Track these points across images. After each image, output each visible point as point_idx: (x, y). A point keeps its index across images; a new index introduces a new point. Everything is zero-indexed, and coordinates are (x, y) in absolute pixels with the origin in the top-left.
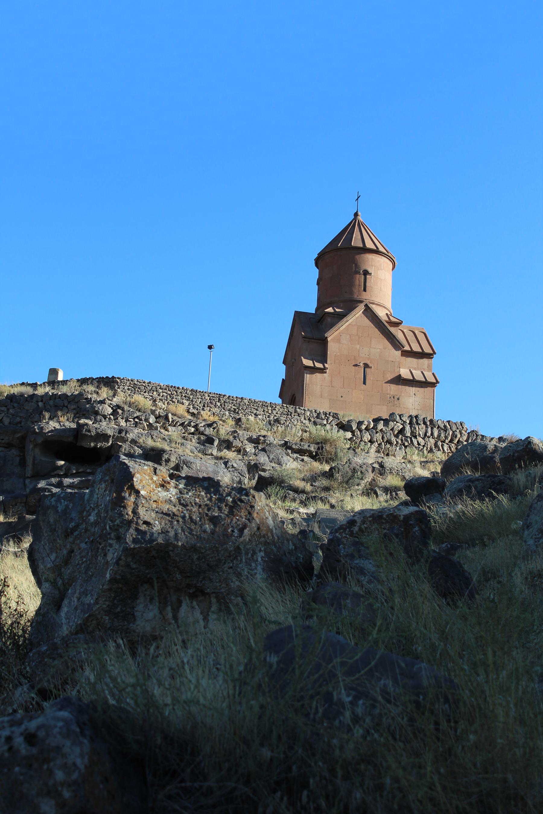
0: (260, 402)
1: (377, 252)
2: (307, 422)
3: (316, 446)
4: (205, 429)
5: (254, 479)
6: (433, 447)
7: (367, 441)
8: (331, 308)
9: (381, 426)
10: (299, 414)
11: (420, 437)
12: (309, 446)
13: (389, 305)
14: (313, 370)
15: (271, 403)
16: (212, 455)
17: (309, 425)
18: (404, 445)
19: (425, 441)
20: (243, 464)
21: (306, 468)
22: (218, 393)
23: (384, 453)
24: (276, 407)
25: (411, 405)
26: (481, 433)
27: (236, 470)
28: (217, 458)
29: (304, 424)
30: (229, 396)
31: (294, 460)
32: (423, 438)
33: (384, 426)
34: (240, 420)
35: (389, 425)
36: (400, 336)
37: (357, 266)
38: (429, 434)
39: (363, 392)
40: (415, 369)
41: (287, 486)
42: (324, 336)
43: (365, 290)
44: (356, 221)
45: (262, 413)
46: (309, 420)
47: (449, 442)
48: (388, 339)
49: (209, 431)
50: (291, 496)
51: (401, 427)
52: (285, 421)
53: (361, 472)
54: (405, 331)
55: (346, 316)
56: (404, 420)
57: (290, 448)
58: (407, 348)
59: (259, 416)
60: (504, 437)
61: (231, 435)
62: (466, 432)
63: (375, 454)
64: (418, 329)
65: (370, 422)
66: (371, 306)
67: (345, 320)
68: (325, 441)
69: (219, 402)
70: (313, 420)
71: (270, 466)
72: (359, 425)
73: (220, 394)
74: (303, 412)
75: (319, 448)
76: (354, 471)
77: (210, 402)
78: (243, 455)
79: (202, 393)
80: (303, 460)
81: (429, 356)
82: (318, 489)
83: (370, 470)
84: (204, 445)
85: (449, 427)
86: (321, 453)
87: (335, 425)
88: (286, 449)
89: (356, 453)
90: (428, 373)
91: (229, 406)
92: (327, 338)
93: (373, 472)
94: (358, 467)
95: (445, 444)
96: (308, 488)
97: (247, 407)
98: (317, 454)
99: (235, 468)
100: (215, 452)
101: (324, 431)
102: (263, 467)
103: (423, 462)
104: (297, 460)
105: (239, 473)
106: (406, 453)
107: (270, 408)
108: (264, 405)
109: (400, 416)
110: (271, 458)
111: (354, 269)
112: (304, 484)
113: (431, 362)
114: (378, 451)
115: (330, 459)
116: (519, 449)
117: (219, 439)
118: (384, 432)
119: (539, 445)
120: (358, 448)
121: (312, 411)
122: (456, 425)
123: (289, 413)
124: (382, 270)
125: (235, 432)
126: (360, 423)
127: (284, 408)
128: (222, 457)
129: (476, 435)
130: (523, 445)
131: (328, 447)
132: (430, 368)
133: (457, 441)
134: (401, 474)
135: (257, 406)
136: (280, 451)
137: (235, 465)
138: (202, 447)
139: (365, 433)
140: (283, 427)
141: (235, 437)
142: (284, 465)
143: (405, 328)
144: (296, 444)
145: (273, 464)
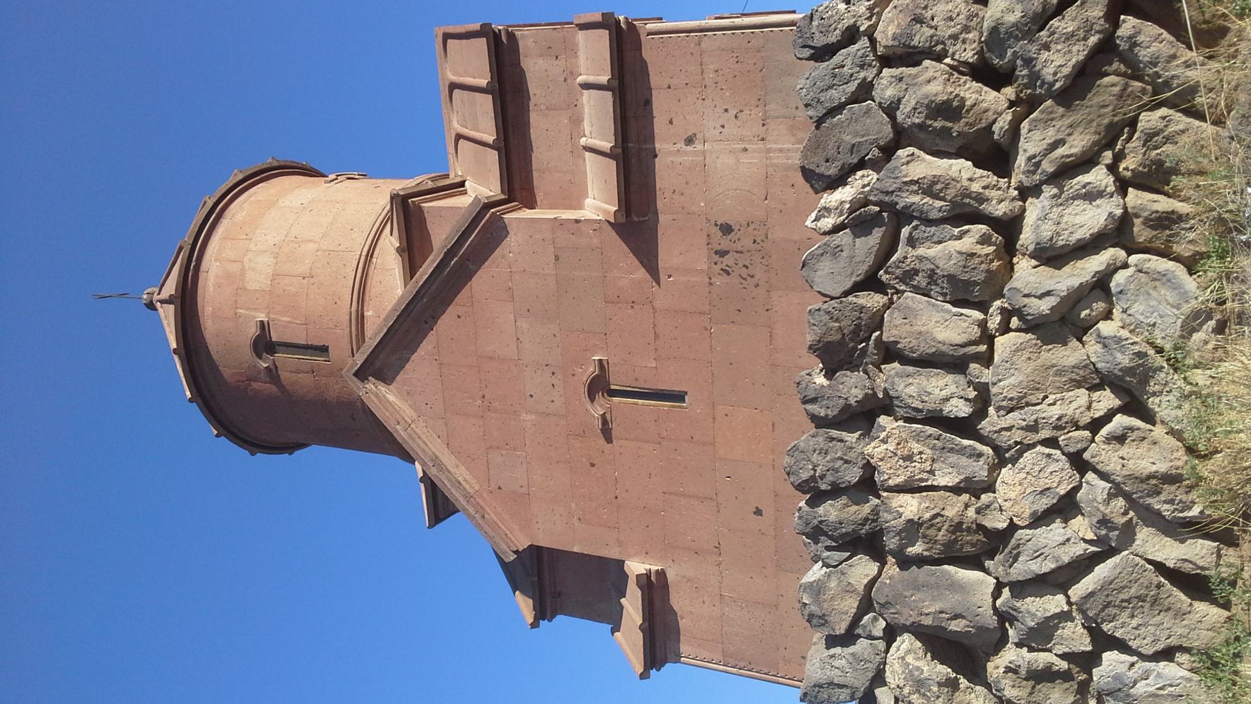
1: (186, 300)
25: (745, 159)
32: (1002, 457)
43: (323, 350)
56: (851, 604)
113: (530, 42)
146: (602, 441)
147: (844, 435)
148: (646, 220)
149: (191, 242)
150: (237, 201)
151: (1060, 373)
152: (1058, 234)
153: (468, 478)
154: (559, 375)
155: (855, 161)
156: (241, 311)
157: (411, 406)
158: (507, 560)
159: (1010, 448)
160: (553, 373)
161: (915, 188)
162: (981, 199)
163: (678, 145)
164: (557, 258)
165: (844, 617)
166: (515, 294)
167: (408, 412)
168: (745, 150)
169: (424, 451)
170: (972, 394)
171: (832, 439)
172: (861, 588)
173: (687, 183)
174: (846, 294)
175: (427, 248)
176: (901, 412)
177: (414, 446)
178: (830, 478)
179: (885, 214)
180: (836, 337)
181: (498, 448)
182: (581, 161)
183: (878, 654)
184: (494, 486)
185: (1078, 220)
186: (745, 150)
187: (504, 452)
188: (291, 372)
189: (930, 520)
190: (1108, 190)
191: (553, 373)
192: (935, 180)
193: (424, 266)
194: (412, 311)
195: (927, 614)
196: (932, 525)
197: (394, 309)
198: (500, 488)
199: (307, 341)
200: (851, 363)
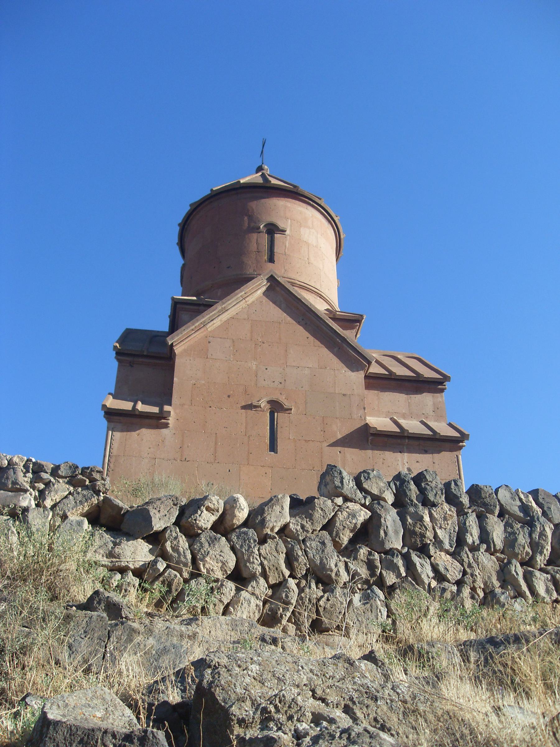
6: (497, 584)
11: (442, 549)
19: (462, 563)
32: (455, 554)
35: (313, 509)
39: (269, 471)
40: (404, 417)
43: (271, 259)
51: (363, 515)
56: (375, 491)
65: (235, 500)
72: (187, 513)
85: (539, 511)
90: (436, 423)
111: (246, 224)
118: (295, 537)
124: (309, 228)
139: (212, 542)
146: (244, 404)
147: (444, 496)
148: (368, 443)
149: (322, 204)
150: (333, 232)
151: (489, 578)
152: (537, 579)
153: (215, 325)
154: (280, 386)
155: (545, 509)
156: (289, 221)
157: (253, 302)
158: (168, 339)
159: (461, 557)
160: (281, 383)
161: (542, 529)
162: (541, 553)
163: (407, 464)
164: (344, 395)
165: (370, 487)
166: (323, 370)
167: (250, 300)
169: (230, 304)
170: (476, 544)
171: (442, 491)
172: (383, 496)
173: (389, 466)
174: (499, 501)
176: (461, 518)
177: (233, 299)
178: (428, 487)
179: (529, 518)
180: (483, 496)
181: (234, 345)
182: (385, 416)
183: (359, 499)
185: (541, 586)
187: (231, 348)
189: (424, 525)
190: (552, 597)
191: (281, 383)
192: (546, 536)
193: (336, 324)
194: (309, 313)
195: (385, 521)
196: (421, 526)
197: (314, 306)
198: (209, 342)
199: (277, 253)
200: (471, 501)
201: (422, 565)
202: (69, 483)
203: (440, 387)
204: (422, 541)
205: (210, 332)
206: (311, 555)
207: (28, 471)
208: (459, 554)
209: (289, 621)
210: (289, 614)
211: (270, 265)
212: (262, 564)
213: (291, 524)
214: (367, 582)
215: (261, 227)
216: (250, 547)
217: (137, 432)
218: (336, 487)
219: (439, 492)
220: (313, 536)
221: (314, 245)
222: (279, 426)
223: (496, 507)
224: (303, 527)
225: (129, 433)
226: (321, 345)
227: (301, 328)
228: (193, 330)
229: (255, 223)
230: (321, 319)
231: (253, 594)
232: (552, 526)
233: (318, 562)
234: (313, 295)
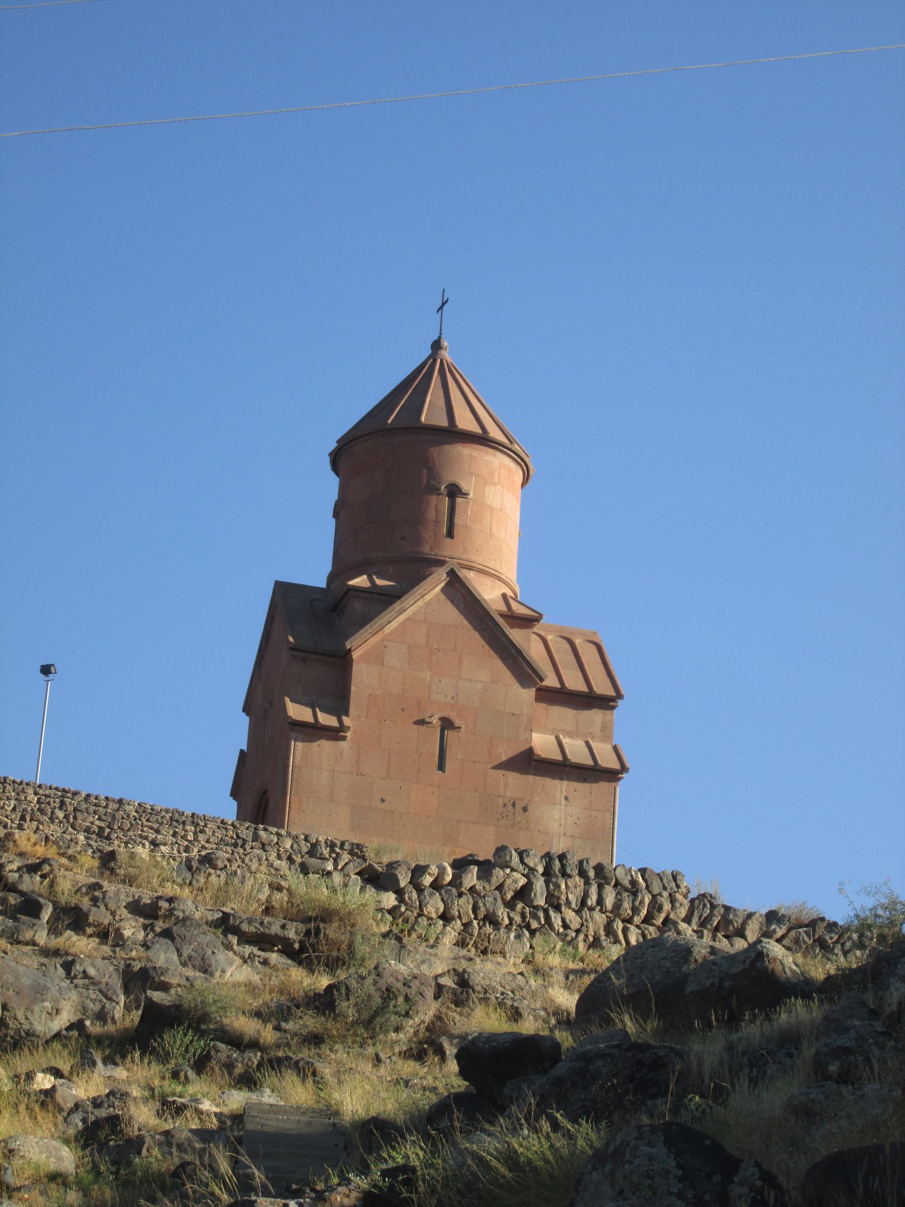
0: (167, 811)
1: (483, 440)
2: (283, 864)
3: (302, 927)
4: (21, 876)
5: (137, 1008)
6: (602, 933)
7: (434, 915)
8: (365, 577)
9: (471, 878)
10: (263, 845)
11: (570, 907)
12: (283, 927)
13: (510, 571)
14: (313, 731)
15: (193, 815)
16: (34, 944)
17: (287, 872)
18: (528, 927)
19: (581, 918)
20: (111, 968)
21: (274, 982)
22: (61, 787)
23: (476, 947)
24: (205, 826)
25: (556, 824)
26: (725, 899)
27: (94, 984)
28: (47, 952)
29: (276, 869)
30: (88, 796)
31: (245, 962)
32: (578, 912)
33: (478, 878)
34: (112, 855)
35: (491, 875)
36: (534, 651)
37: (434, 474)
38: (592, 900)
40: (570, 735)
41: (215, 1030)
42: (344, 647)
43: (450, 534)
44: (435, 361)
45: (171, 839)
46: (290, 859)
47: (643, 922)
48: (504, 659)
49: (31, 884)
50: (223, 1056)
51: (523, 881)
52: (229, 860)
53: (407, 999)
54: (549, 638)
55: (399, 597)
56: (531, 865)
57: (236, 931)
58: (551, 681)
59: (162, 848)
60: (783, 911)
61: (87, 893)
62: (685, 896)
63: (451, 950)
64: (582, 634)
65: (444, 869)
66: (464, 574)
67: (397, 608)
68: (326, 915)
69: (61, 808)
70: (298, 859)
71: (181, 975)
73: (64, 790)
74: (275, 840)
75: (308, 933)
76: (388, 994)
77: (39, 810)
78: (113, 946)
79: (20, 787)
80: (265, 962)
81: (606, 703)
82: (292, 1039)
83: (430, 993)
84: (15, 919)
86: (313, 945)
87: (357, 874)
88: (225, 933)
89: (403, 947)
91: (85, 820)
92: (349, 651)
93: (437, 997)
94: (399, 985)
95: (632, 928)
96: (268, 1035)
97: (132, 825)
98: (303, 949)
99: (90, 978)
100: (42, 937)
101: (325, 890)
102: (162, 978)
103: (573, 971)
104: (253, 961)
105: (100, 991)
106: (531, 947)
107: (188, 828)
108: (176, 819)
109: (521, 854)
110: (185, 955)
112: (258, 1027)
113: (609, 717)
114: (461, 943)
115: (337, 959)
116: (734, 970)
117: (55, 904)
118: (478, 894)
119: (785, 962)
120: (409, 935)
121: (297, 837)
122: (662, 881)
123: (240, 842)
124: (494, 484)
125: (98, 887)
126: (418, 871)
127: (226, 829)
128: (58, 950)
129: (712, 905)
130: (744, 962)
131: (331, 931)
132: (606, 733)
133: (661, 920)
134: (509, 1002)
135: (157, 821)
136: (210, 937)
137: (92, 972)
138: (10, 923)
139: (431, 895)
140: (223, 875)
141: (95, 901)
142: (218, 974)
143: (550, 632)
144: (250, 921)
145: (190, 972)
146: (416, 719)
157: (431, 599)
162: (638, 915)
164: (513, 714)
168: (561, 825)
172: (537, 868)
175: (512, 626)
184: (387, 643)
186: (561, 825)
187: (407, 655)
188: (436, 506)
200: (596, 874)
201: (555, 918)
202: (349, 853)
203: (611, 704)
204: (558, 901)
205: (387, 635)
206: (488, 906)
207: (327, 846)
208: (581, 912)
209: (472, 946)
210: (472, 942)
211: (448, 540)
212: (459, 911)
213: (477, 887)
214: (519, 926)
215: (442, 488)
216: (452, 900)
217: (318, 742)
218: (507, 861)
219: (575, 868)
220: (489, 894)
221: (499, 507)
222: (448, 747)
223: (612, 880)
224: (484, 887)
225: (310, 744)
226: (496, 656)
227: (476, 635)
228: (370, 633)
229: (435, 480)
230: (499, 626)
231: (453, 929)
232: (650, 896)
233: (492, 911)
234: (492, 578)
